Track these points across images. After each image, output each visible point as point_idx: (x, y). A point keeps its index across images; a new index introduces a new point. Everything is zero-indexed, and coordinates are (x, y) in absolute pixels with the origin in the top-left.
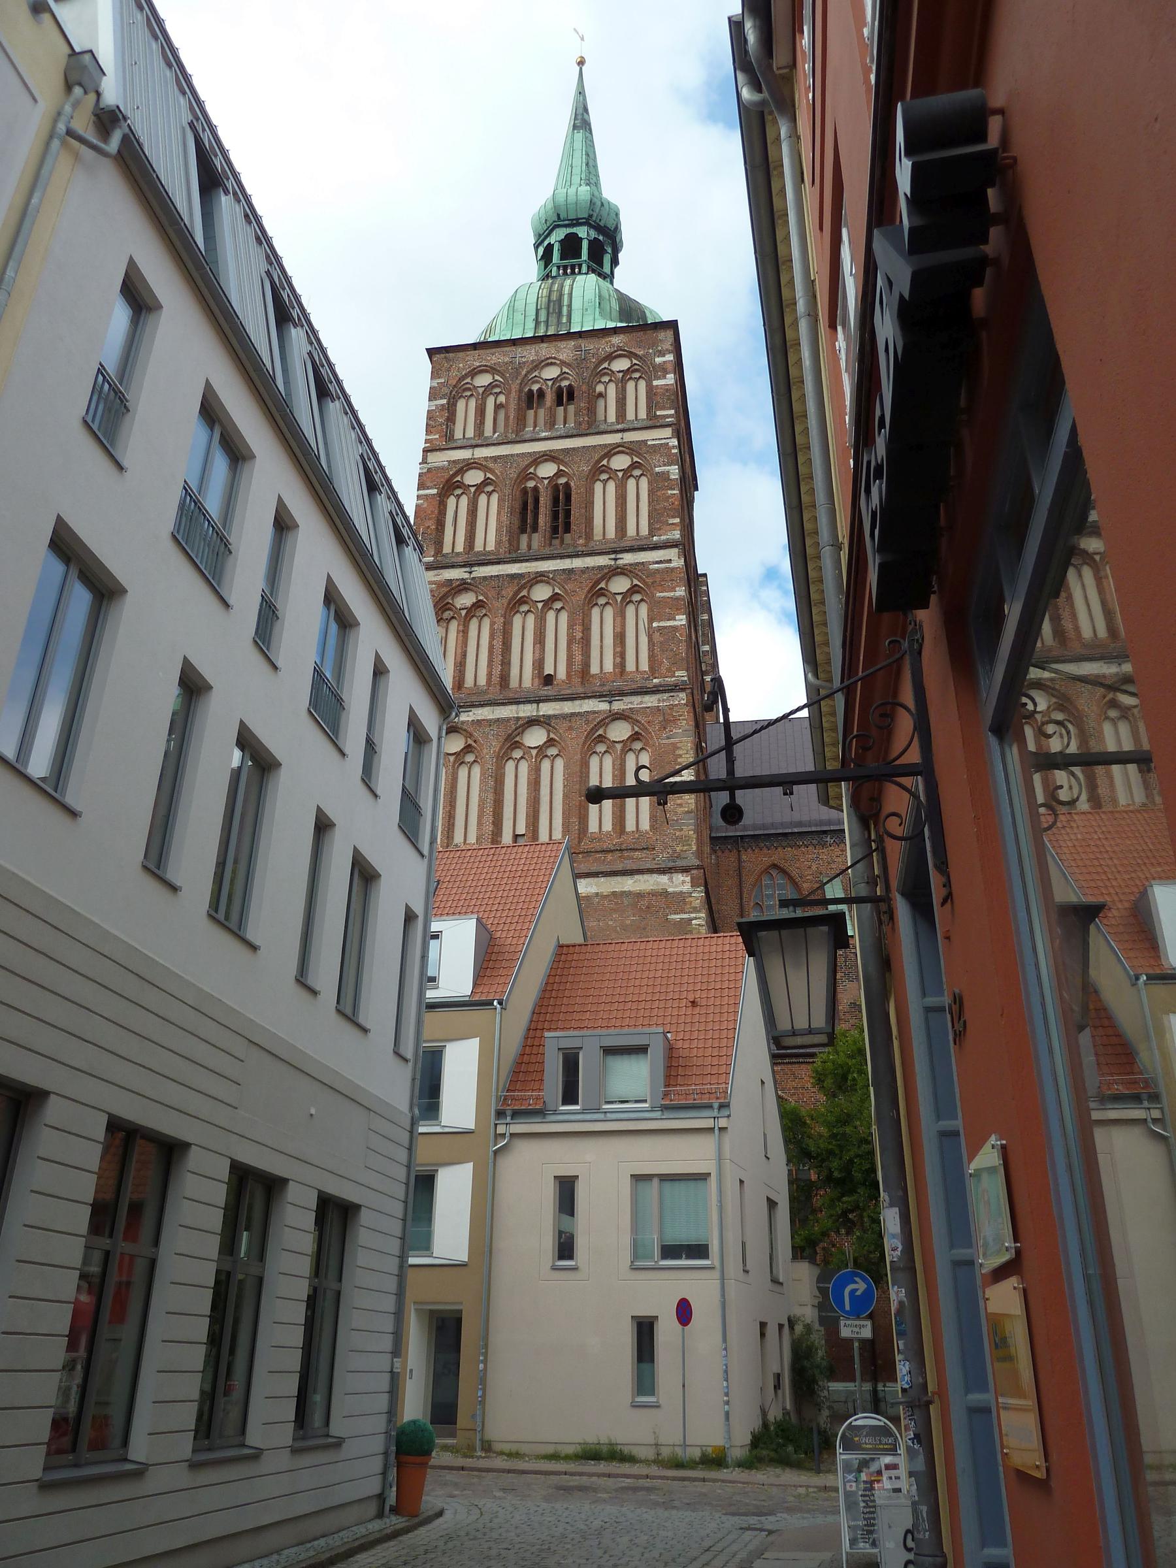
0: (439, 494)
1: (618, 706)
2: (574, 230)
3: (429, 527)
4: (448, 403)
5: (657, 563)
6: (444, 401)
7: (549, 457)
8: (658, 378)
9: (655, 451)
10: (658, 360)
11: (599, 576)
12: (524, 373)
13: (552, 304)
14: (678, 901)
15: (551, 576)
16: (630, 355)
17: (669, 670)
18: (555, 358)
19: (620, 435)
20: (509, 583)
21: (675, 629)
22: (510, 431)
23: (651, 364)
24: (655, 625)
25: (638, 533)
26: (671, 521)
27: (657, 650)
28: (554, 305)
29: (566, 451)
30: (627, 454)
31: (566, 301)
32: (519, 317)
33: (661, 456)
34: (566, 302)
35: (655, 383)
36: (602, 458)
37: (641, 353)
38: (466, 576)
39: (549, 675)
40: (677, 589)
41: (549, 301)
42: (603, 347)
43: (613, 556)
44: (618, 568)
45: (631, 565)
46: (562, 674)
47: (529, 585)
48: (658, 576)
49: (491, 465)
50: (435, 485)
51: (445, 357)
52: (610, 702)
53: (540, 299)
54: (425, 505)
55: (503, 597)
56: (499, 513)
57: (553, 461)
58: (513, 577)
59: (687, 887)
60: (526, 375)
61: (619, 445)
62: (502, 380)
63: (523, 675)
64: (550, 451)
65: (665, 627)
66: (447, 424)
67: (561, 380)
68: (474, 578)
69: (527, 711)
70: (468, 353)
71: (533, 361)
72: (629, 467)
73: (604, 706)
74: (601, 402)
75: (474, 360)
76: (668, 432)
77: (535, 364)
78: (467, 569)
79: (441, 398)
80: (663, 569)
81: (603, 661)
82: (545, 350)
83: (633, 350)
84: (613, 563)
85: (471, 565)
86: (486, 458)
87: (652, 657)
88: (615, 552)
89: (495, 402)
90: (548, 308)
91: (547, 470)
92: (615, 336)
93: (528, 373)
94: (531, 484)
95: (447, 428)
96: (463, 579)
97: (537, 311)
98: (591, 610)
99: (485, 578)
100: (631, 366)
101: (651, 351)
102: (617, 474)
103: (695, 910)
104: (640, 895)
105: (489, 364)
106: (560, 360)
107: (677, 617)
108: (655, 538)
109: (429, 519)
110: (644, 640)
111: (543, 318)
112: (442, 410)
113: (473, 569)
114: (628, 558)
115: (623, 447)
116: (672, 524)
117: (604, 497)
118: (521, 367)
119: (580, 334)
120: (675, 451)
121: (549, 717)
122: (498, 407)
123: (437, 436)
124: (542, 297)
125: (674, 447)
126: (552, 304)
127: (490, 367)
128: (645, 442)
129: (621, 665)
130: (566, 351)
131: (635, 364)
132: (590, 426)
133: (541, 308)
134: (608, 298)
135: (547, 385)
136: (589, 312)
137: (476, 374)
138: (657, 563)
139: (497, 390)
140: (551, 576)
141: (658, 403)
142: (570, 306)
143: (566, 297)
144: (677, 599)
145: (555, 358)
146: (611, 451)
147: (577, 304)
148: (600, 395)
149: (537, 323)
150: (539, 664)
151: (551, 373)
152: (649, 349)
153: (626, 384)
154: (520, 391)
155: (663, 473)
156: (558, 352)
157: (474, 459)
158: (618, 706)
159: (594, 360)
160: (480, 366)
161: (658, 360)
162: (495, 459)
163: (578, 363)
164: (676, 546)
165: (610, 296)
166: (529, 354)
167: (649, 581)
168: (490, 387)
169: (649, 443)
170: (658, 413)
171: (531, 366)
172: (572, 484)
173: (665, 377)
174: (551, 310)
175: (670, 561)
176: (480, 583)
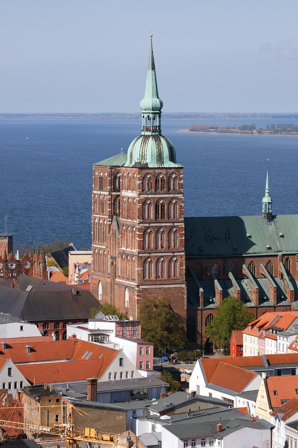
1: (175, 254)
5: (180, 226)
6: (141, 181)
7: (161, 198)
8: (180, 181)
10: (181, 176)
14: (183, 288)
16: (176, 174)
17: (182, 248)
21: (183, 239)
29: (165, 198)
32: (154, 158)
34: (162, 155)
35: (180, 182)
38: (149, 225)
58: (157, 226)
69: (160, 254)
73: (172, 254)
76: (182, 195)
82: (160, 171)
88: (173, 223)
103: (185, 290)
104: (178, 287)
111: (158, 159)
112: (141, 184)
114: (176, 224)
125: (183, 199)
130: (164, 171)
132: (168, 191)
142: (163, 156)
143: (162, 153)
144: (183, 233)
147: (164, 156)
151: (161, 176)
158: (175, 254)
163: (166, 174)
166: (157, 171)
169: (179, 197)
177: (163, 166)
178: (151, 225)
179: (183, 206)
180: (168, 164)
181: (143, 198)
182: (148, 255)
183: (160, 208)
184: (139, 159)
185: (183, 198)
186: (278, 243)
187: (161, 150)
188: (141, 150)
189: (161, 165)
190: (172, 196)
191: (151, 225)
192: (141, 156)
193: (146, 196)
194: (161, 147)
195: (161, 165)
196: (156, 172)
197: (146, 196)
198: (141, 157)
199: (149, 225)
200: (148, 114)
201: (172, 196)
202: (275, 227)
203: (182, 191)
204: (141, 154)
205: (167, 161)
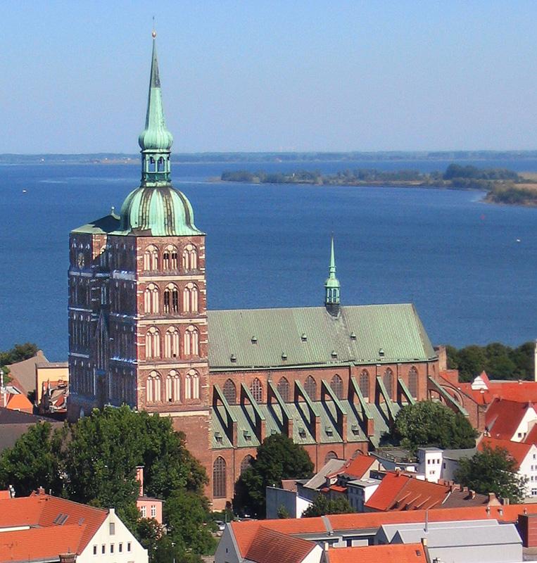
2: (163, 155)
10: (201, 248)
16: (193, 244)
35: (200, 257)
46: (178, 355)
59: (208, 414)
63: (168, 354)
76: (203, 277)
81: (187, 352)
87: (199, 351)
91: (171, 286)
110: (197, 346)
114: (194, 321)
117: (186, 295)
129: (191, 353)
146: (188, 281)
147: (176, 219)
150: (172, 352)
161: (201, 248)
162: (158, 281)
177: (174, 234)
178: (158, 322)
179: (205, 294)
180: (181, 229)
182: (152, 367)
183: (171, 297)
184: (137, 221)
186: (349, 348)
187: (170, 210)
188: (141, 209)
189: (172, 232)
190: (189, 278)
191: (158, 322)
192: (141, 218)
193: (149, 279)
194: (171, 205)
195: (172, 232)
197: (149, 279)
198: (141, 220)
200: (151, 155)
201: (189, 278)
202: (345, 323)
204: (141, 215)
205: (180, 225)
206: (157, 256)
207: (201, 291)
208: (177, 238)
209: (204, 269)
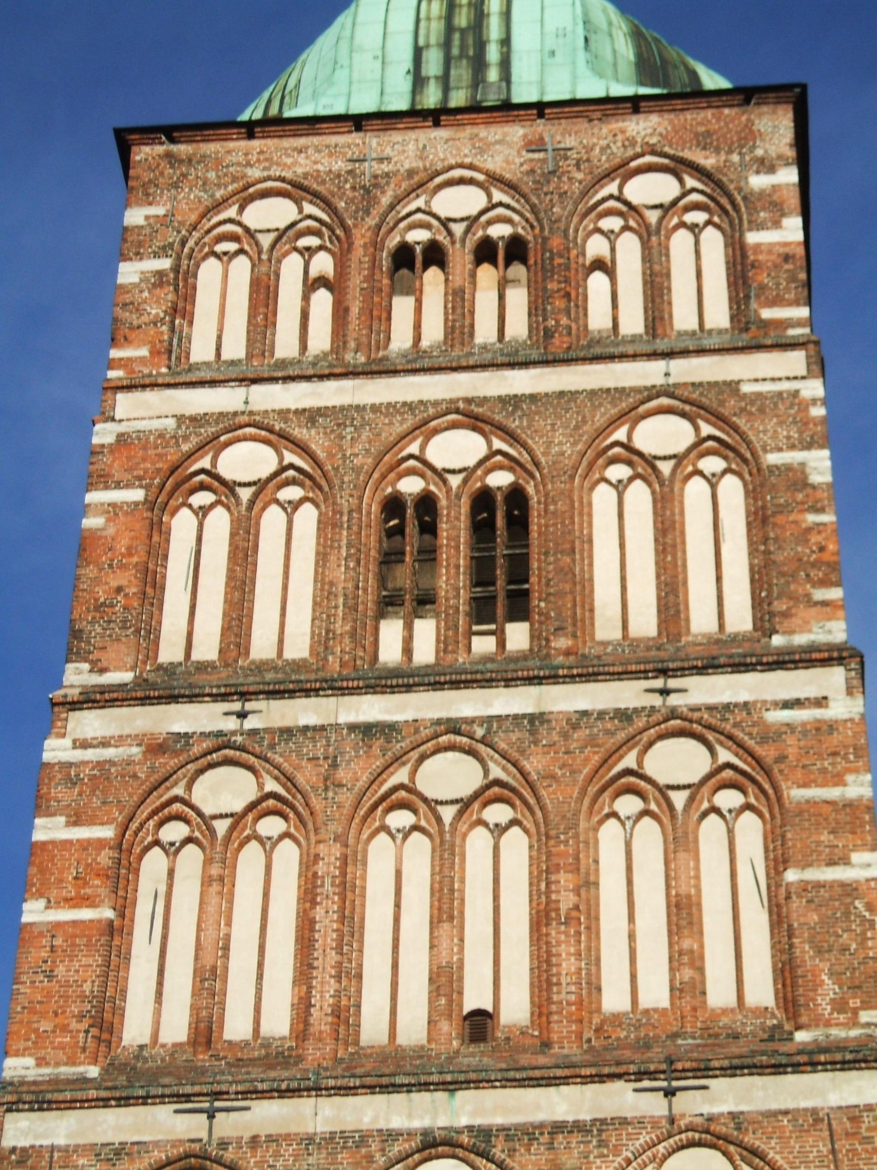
0: (150, 504)
3: (119, 590)
4: (176, 269)
5: (787, 705)
6: (165, 264)
8: (760, 226)
9: (762, 410)
10: (758, 182)
11: (622, 736)
12: (385, 200)
13: (457, 36)
15: (480, 732)
17: (840, 1005)
18: (471, 167)
19: (660, 365)
20: (356, 749)
21: (849, 890)
22: (352, 344)
23: (740, 190)
24: (791, 876)
25: (721, 626)
26: (820, 594)
27: (804, 950)
28: (462, 40)
29: (513, 402)
30: (683, 415)
31: (494, 30)
33: (781, 423)
36: (614, 423)
37: (708, 161)
38: (232, 724)
39: (479, 1013)
40: (850, 778)
41: (450, 28)
42: (603, 143)
43: (658, 683)
44: (673, 714)
45: (711, 708)
47: (415, 755)
48: (791, 740)
49: (299, 432)
50: (140, 478)
51: (168, 155)
52: (670, 1093)
53: (423, 24)
54: (111, 531)
55: (340, 785)
56: (322, 558)
57: (474, 429)
60: (392, 207)
61: (654, 393)
62: (324, 217)
64: (468, 401)
65: (819, 885)
66: (172, 322)
67: (490, 223)
68: (254, 732)
70: (231, 145)
71: (411, 173)
72: (689, 450)
74: (598, 282)
75: (249, 164)
77: (416, 179)
78: (237, 706)
79: (156, 255)
80: (804, 724)
83: (687, 154)
84: (656, 700)
85: (245, 696)
86: (283, 414)
88: (664, 672)
89: (306, 272)
90: (446, 45)
92: (635, 118)
93: (399, 200)
94: (411, 486)
95: (172, 330)
96: (220, 734)
97: (418, 53)
98: (596, 830)
99: (287, 732)
100: (684, 195)
101: (735, 158)
102: (654, 468)
105: (288, 175)
106: (487, 173)
107: (855, 857)
108: (777, 640)
109: (122, 567)
113: (249, 706)
115: (672, 396)
116: (825, 603)
118: (376, 186)
119: (540, 109)
120: (818, 412)
121: (485, 1133)
122: (311, 285)
123: (144, 352)
124: (429, 19)
125: (814, 401)
126: (457, 36)
127: (290, 183)
128: (732, 387)
131: (694, 190)
133: (428, 46)
134: (604, 26)
135: (450, 233)
136: (559, 58)
137: (252, 199)
138: (787, 705)
139: (312, 241)
140: (480, 732)
141: (762, 288)
142: (506, 42)
144: (850, 806)
145: (471, 167)
148: (599, 265)
149: (418, 81)
152: (730, 152)
153: (668, 238)
154: (376, 245)
155: (789, 468)
156: (482, 151)
157: (251, 413)
159: (580, 176)
160: (266, 179)
161: (758, 182)
162: (311, 416)
164: (840, 661)
165: (610, 24)
167: (768, 753)
168: (291, 233)
169: (746, 388)
170: (767, 314)
171: (404, 185)
172: (530, 489)
173: (777, 224)
174: (455, 51)
175: (821, 702)
176: (272, 746)
181: (171, 423)
185: (814, 388)
196: (385, 167)
199: (242, 715)
203: (799, 323)
206: (323, 264)
207: (772, 458)
208: (516, 132)
209: (803, 312)
